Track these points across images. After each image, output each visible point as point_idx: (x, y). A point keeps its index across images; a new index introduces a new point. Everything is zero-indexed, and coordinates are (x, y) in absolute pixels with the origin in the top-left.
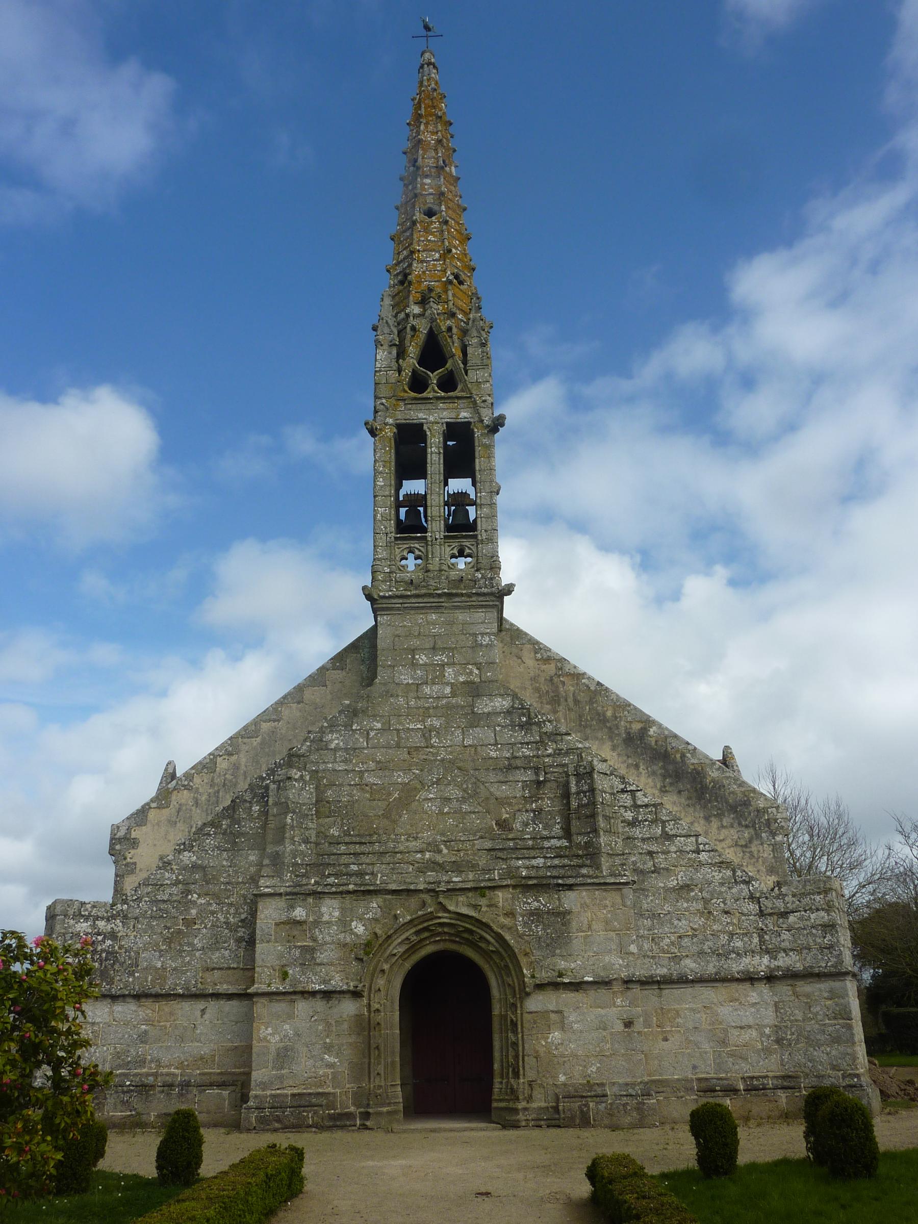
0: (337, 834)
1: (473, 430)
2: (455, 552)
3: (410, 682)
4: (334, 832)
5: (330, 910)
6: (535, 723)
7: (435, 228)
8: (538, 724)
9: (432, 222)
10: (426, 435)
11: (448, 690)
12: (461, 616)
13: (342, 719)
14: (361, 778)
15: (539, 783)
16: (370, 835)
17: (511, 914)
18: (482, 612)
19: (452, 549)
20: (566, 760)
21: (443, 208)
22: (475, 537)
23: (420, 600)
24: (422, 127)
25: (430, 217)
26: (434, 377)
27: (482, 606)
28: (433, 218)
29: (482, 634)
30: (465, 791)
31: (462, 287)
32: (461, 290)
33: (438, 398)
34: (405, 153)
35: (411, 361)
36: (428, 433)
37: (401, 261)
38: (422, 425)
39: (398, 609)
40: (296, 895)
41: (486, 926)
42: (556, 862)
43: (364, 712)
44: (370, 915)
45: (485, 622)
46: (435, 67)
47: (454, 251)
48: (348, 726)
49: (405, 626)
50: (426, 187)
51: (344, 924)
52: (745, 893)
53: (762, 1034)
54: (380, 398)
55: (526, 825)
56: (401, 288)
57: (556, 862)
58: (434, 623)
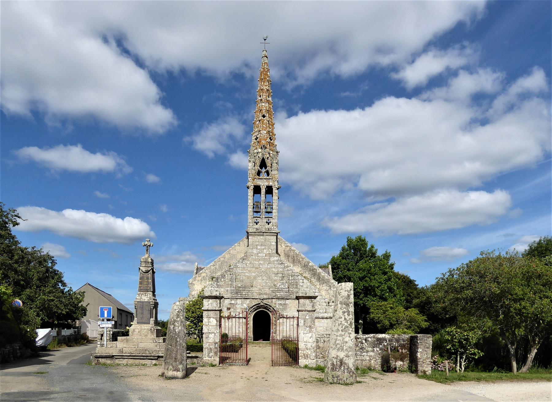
0: (240, 286)
3: (256, 253)
4: (239, 285)
5: (239, 301)
6: (283, 263)
7: (265, 122)
8: (284, 264)
9: (264, 120)
11: (264, 255)
12: (268, 237)
13: (241, 261)
14: (245, 274)
15: (283, 277)
16: (247, 286)
17: (275, 304)
20: (289, 272)
21: (268, 115)
23: (259, 233)
25: (264, 118)
27: (273, 235)
28: (265, 118)
29: (273, 242)
30: (267, 278)
35: (257, 168)
38: (260, 186)
39: (254, 235)
40: (232, 299)
41: (271, 306)
42: (286, 294)
43: (246, 259)
44: (247, 303)
46: (267, 57)
48: (242, 262)
50: (263, 107)
51: (242, 304)
52: (324, 301)
53: (324, 328)
55: (280, 285)
57: (286, 294)
58: (262, 239)
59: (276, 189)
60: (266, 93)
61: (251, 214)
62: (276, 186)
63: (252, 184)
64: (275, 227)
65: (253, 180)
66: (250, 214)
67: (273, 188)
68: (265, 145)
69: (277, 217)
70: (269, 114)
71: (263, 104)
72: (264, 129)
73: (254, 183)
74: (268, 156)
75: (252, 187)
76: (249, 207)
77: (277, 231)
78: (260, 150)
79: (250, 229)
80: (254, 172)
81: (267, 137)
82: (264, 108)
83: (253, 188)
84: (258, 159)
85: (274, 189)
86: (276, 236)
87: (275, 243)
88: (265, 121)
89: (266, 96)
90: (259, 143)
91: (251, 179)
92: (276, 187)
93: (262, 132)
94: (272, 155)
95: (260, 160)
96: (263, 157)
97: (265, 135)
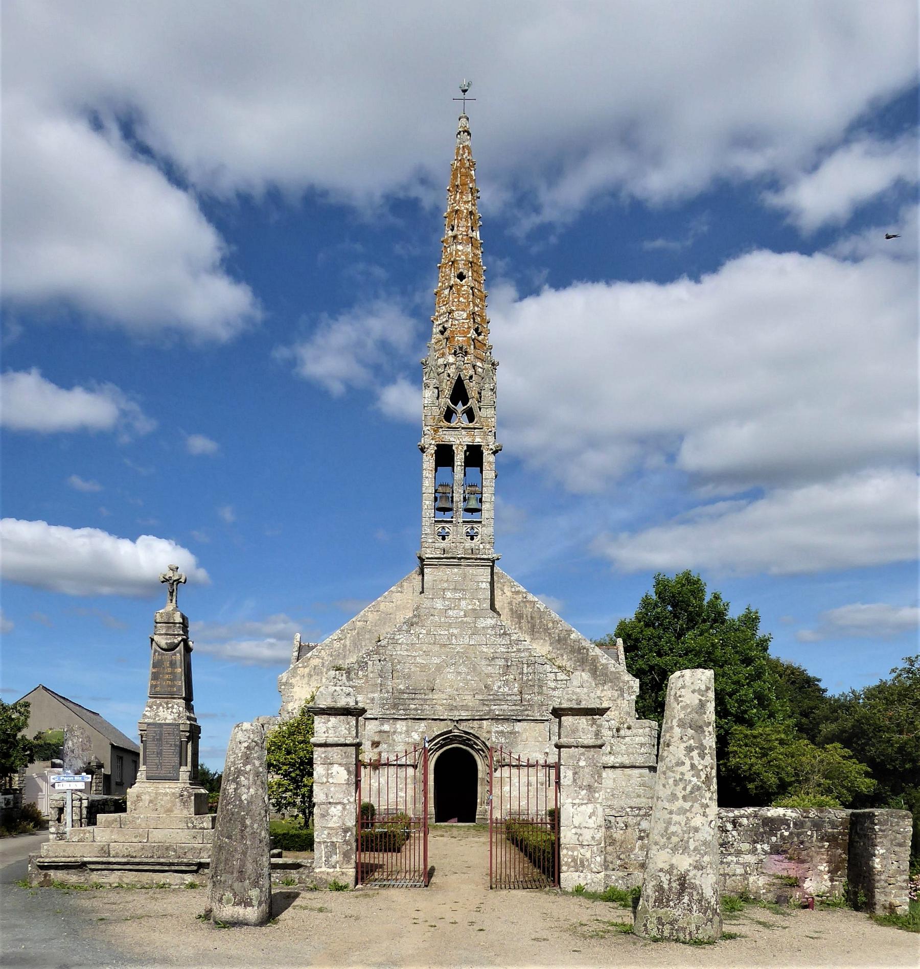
9: (462, 286)
10: (454, 453)
12: (471, 570)
27: (482, 566)
36: (455, 452)
39: (436, 565)
50: (460, 253)
62: (491, 447)
63: (433, 442)
65: (436, 431)
66: (428, 514)
67: (484, 451)
68: (465, 347)
69: (492, 521)
74: (471, 372)
75: (432, 450)
78: (451, 359)
79: (428, 551)
80: (436, 412)
82: (462, 257)
87: (488, 584)
91: (429, 428)
92: (492, 449)
93: (456, 314)
96: (460, 375)
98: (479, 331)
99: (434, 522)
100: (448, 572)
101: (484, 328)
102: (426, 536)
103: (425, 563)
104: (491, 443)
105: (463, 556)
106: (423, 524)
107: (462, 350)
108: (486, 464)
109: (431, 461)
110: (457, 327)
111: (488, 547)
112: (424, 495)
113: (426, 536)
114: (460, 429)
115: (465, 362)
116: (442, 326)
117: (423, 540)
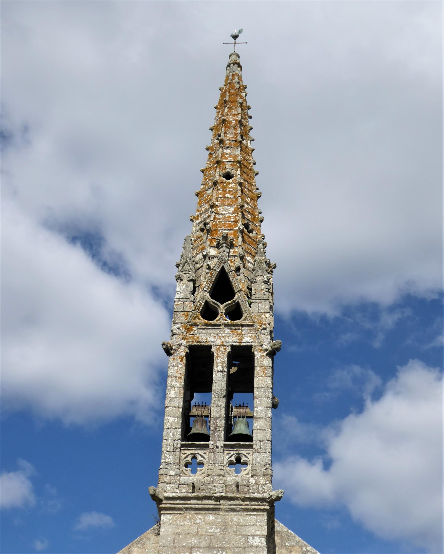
1: (253, 353)
2: (233, 459)
7: (231, 188)
9: (229, 184)
10: (213, 356)
12: (235, 517)
18: (254, 515)
19: (231, 457)
21: (239, 172)
22: (251, 447)
24: (226, 110)
26: (222, 308)
27: (254, 510)
28: (231, 180)
29: (253, 536)
31: (251, 235)
32: (250, 238)
33: (226, 325)
34: (211, 129)
36: (215, 354)
37: (203, 212)
38: (210, 347)
39: (180, 509)
45: (256, 525)
47: (246, 206)
49: (184, 525)
50: (226, 156)
54: (177, 323)
56: (201, 234)
58: (211, 524)
59: (265, 354)
60: (235, 128)
61: (174, 435)
62: (265, 347)
63: (184, 343)
64: (262, 480)
65: (188, 330)
66: (171, 434)
67: (256, 353)
68: (230, 237)
69: (269, 445)
70: (242, 172)
71: (227, 151)
72: (226, 203)
73: (190, 340)
74: (238, 263)
75: (182, 352)
76: (166, 413)
77: (271, 493)
78: (213, 252)
80: (190, 307)
81: (236, 221)
82: (229, 159)
83: (187, 353)
84: (207, 273)
85: (258, 355)
86: (265, 513)
87: (263, 540)
88: (229, 186)
89: (235, 134)
90: (212, 235)
91: (179, 325)
92: (267, 350)
93: (220, 209)
94: (250, 265)
95: (211, 274)
96: (223, 267)
97: (230, 215)
98: (250, 228)
99: (179, 446)
100: (199, 521)
101: (257, 226)
102: (166, 466)
103: (161, 506)
104: (266, 343)
105: (223, 494)
106: (163, 449)
107: (226, 240)
108: (258, 368)
109: (180, 366)
110: (221, 220)
111: (262, 482)
112: (168, 409)
113: (166, 466)
114: (223, 326)
115: (231, 254)
116: (203, 223)
117: (161, 472)
